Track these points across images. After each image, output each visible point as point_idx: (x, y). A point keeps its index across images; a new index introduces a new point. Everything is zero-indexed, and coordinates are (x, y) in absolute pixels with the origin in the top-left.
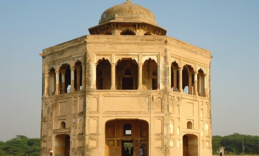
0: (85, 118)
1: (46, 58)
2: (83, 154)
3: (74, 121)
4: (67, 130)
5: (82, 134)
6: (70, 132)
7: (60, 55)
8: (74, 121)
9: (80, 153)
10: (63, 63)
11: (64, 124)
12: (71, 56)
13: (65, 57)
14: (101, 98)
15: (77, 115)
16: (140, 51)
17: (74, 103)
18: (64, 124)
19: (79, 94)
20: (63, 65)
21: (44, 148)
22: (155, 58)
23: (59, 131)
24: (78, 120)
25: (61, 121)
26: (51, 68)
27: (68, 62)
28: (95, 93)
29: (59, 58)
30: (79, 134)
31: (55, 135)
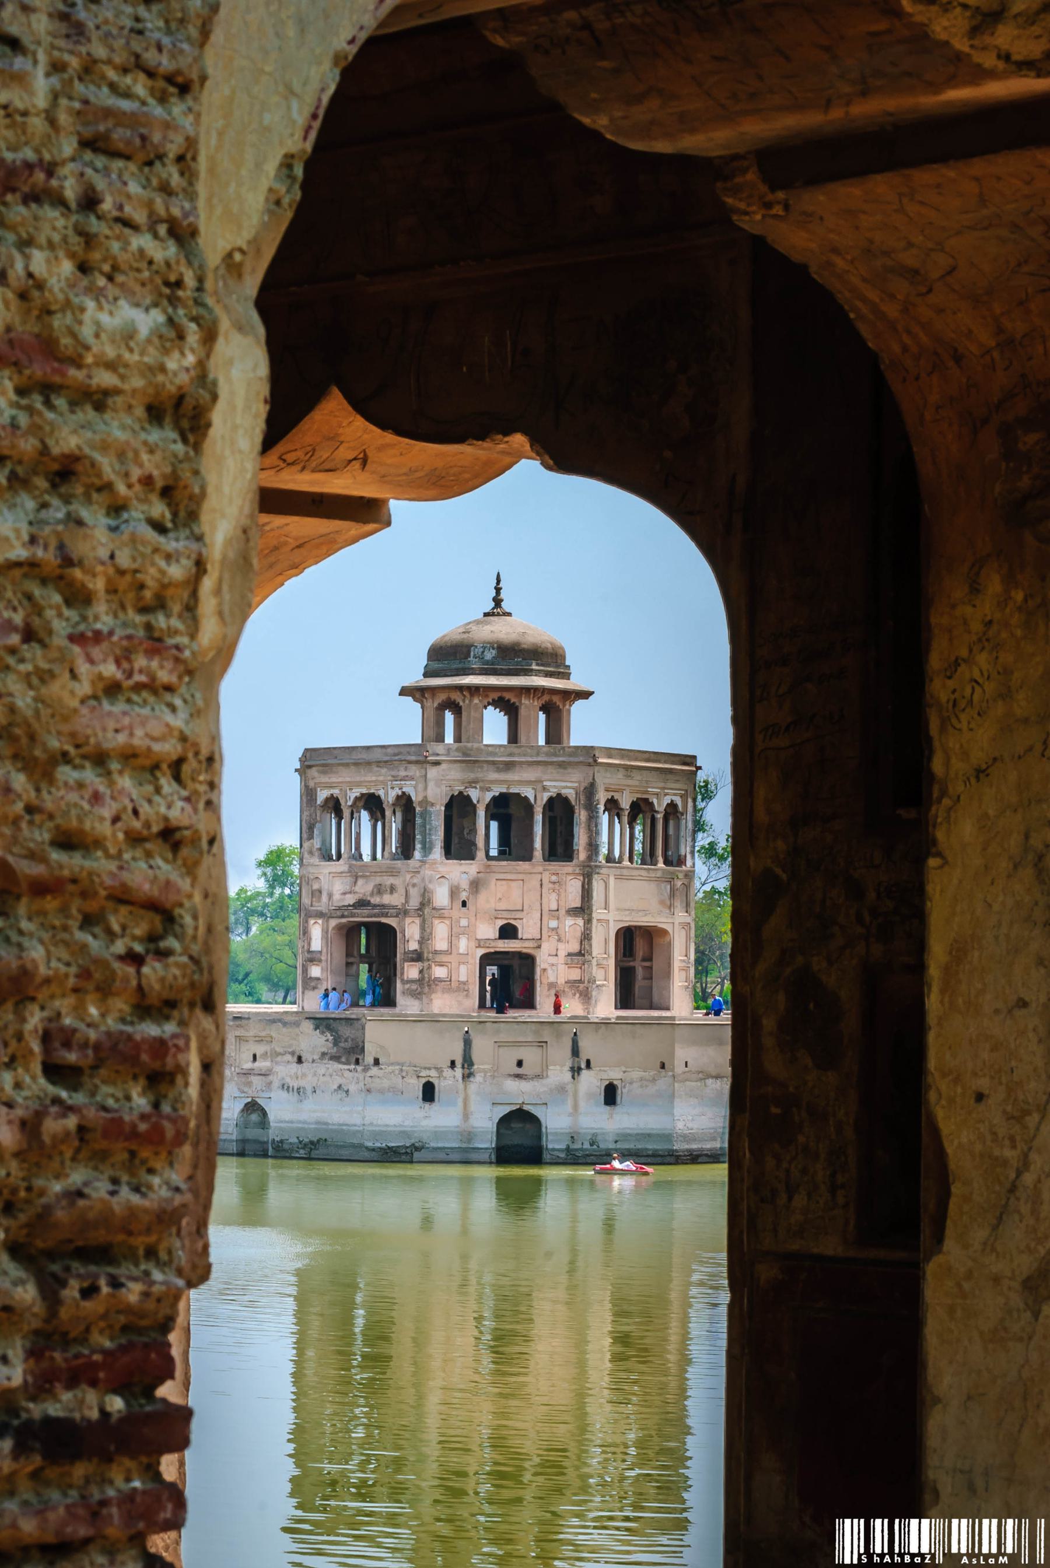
0: (589, 921)
1: (444, 766)
2: (586, 995)
3: (553, 924)
4: (531, 944)
5: (580, 954)
6: (539, 947)
7: (499, 770)
8: (553, 924)
9: (574, 995)
10: (504, 791)
11: (508, 932)
12: (542, 782)
13: (516, 778)
14: (612, 881)
15: (562, 912)
16: (662, 785)
17: (551, 885)
18: (508, 932)
19: (570, 869)
20: (501, 794)
21: (439, 980)
22: (678, 801)
23: (493, 944)
24: (573, 926)
25: (500, 923)
26: (456, 794)
27: (528, 793)
28: (604, 871)
29: (493, 776)
30: (569, 955)
31: (481, 952)
